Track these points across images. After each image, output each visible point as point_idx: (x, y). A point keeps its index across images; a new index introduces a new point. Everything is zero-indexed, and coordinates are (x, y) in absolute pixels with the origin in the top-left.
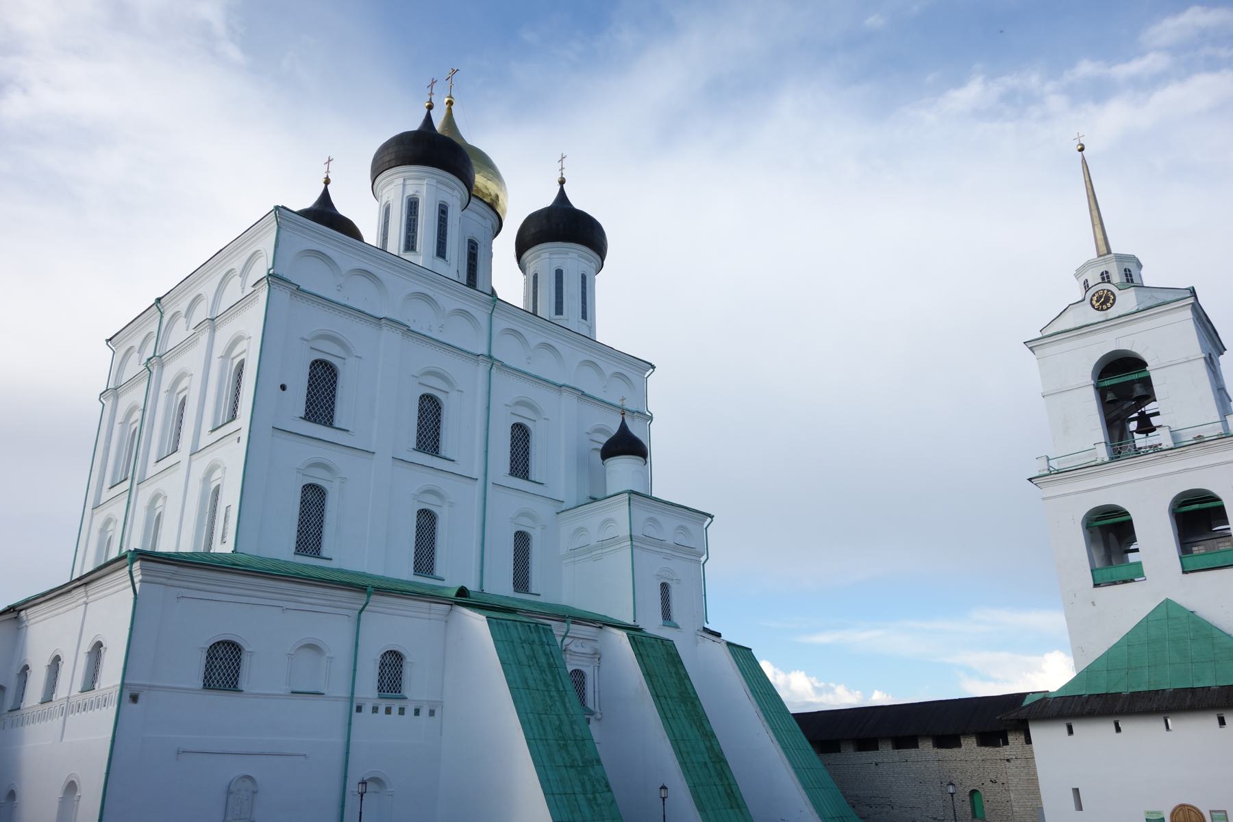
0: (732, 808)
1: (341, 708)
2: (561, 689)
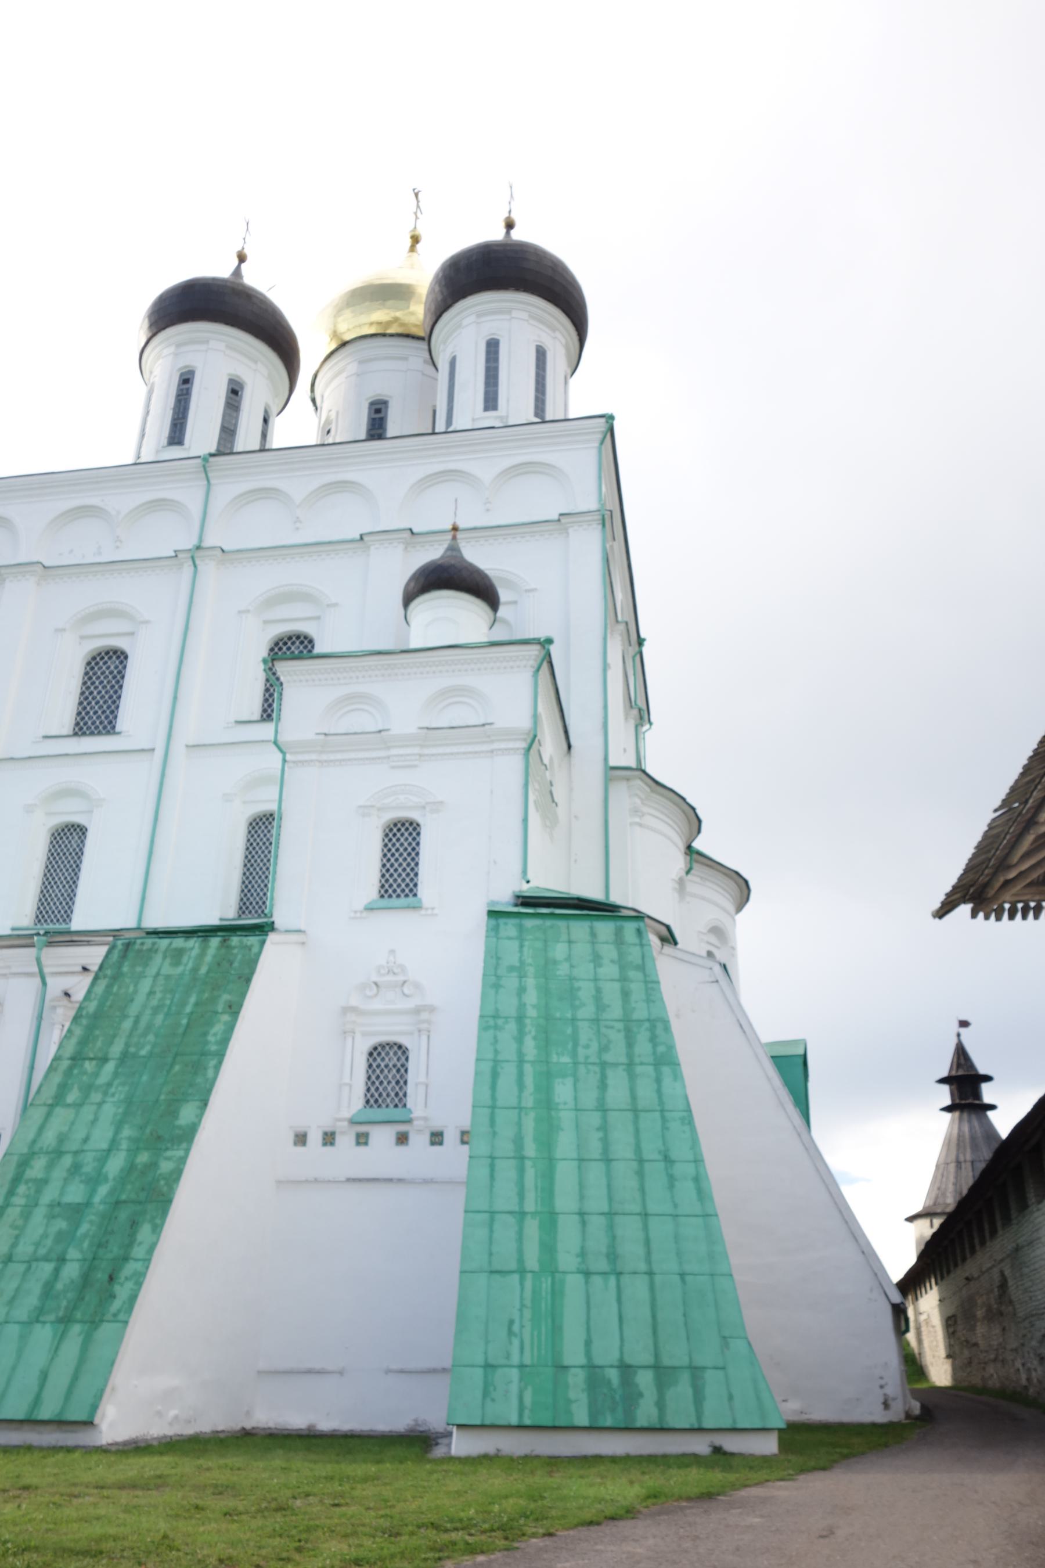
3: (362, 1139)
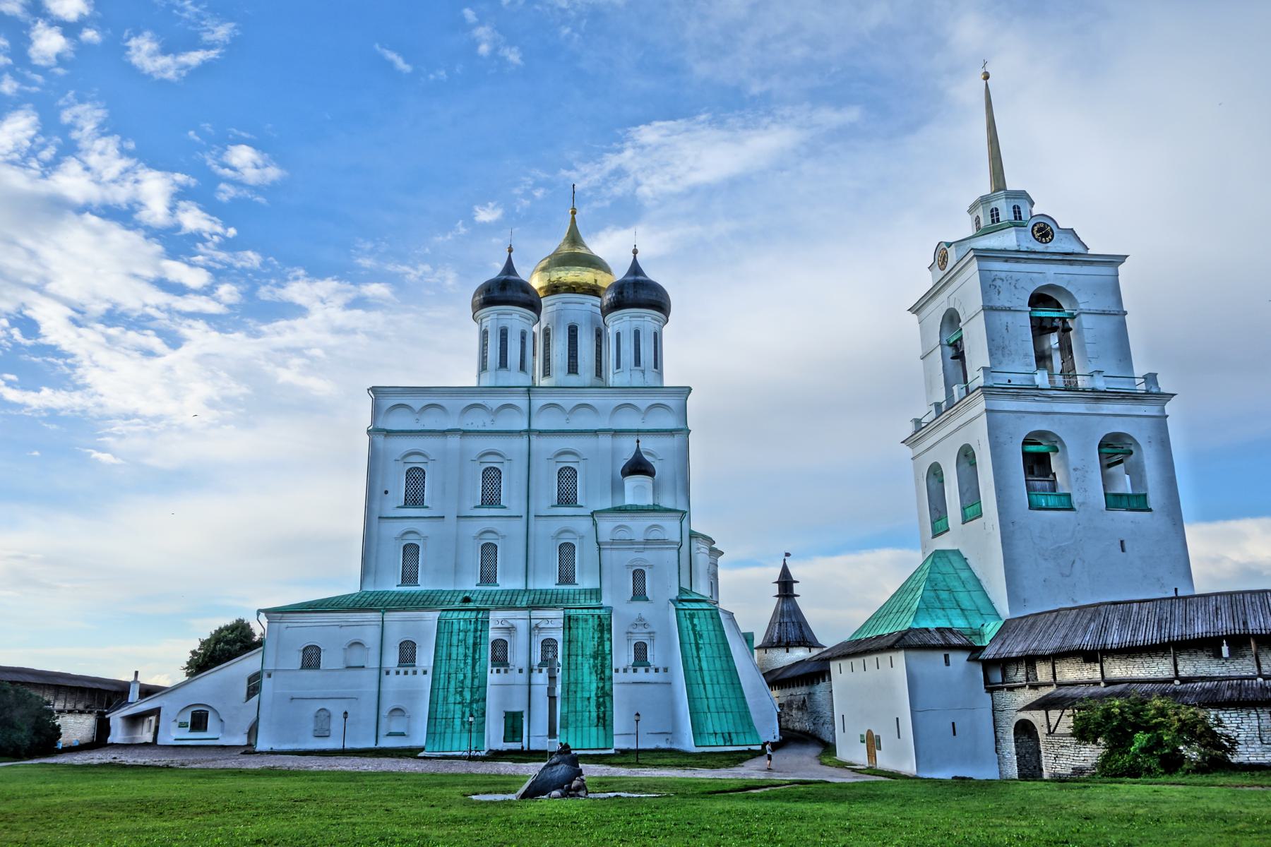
0: (597, 726)
1: (376, 672)
2: (477, 657)
3: (635, 671)
